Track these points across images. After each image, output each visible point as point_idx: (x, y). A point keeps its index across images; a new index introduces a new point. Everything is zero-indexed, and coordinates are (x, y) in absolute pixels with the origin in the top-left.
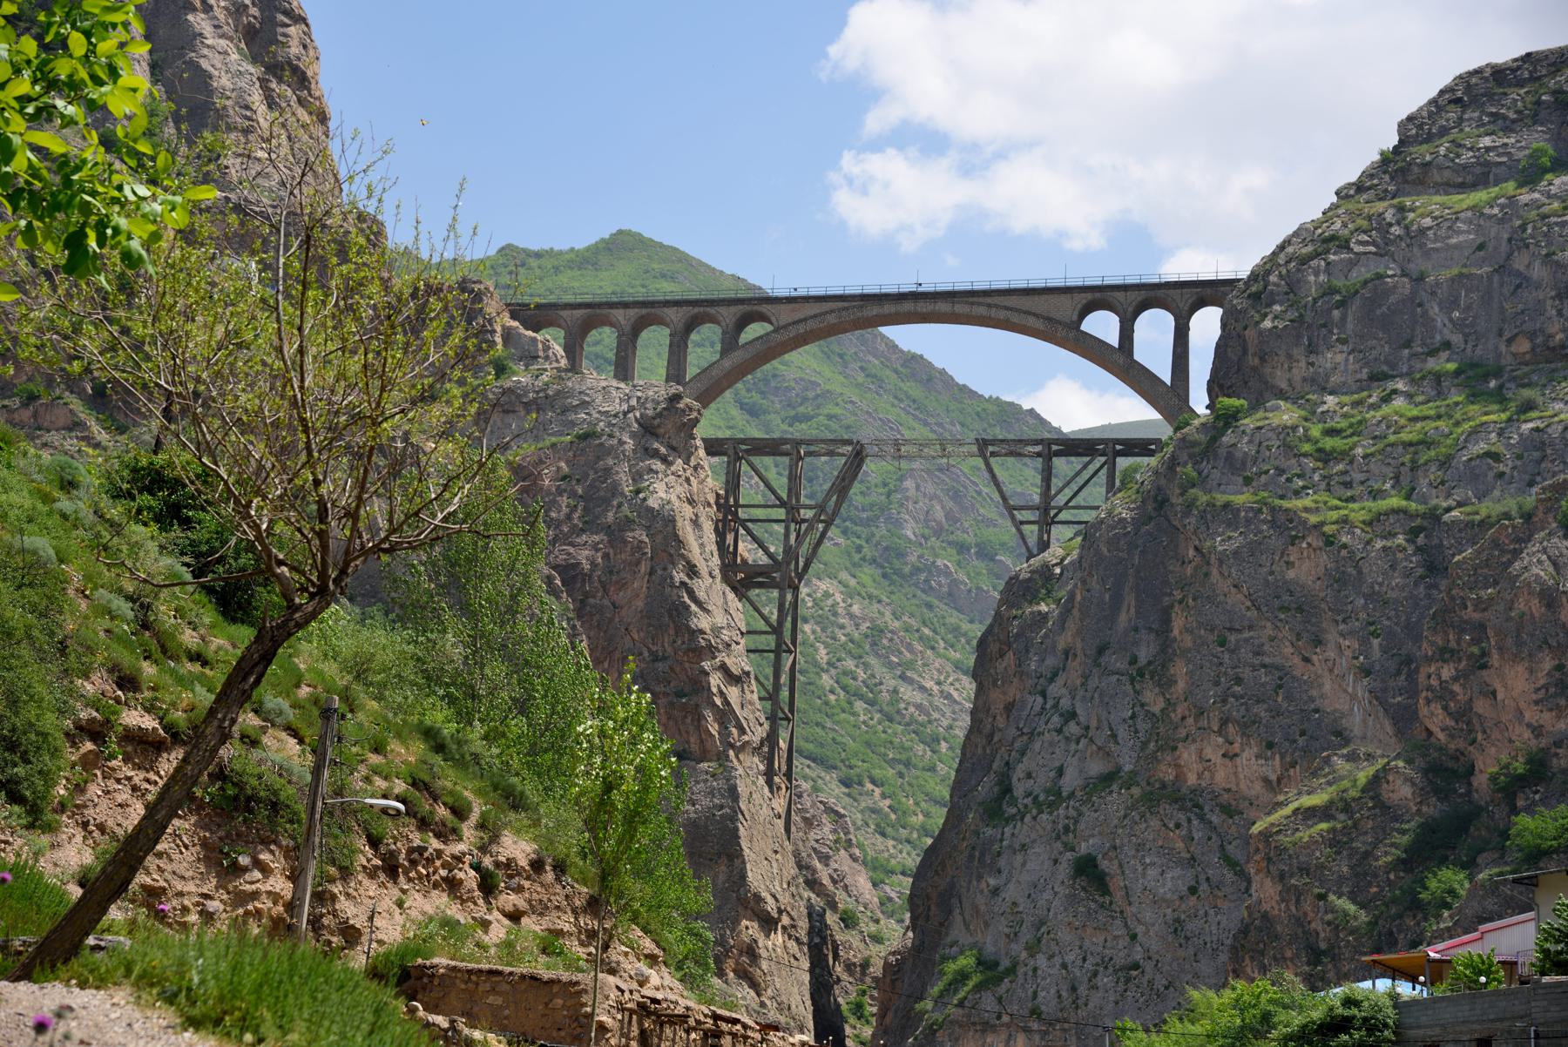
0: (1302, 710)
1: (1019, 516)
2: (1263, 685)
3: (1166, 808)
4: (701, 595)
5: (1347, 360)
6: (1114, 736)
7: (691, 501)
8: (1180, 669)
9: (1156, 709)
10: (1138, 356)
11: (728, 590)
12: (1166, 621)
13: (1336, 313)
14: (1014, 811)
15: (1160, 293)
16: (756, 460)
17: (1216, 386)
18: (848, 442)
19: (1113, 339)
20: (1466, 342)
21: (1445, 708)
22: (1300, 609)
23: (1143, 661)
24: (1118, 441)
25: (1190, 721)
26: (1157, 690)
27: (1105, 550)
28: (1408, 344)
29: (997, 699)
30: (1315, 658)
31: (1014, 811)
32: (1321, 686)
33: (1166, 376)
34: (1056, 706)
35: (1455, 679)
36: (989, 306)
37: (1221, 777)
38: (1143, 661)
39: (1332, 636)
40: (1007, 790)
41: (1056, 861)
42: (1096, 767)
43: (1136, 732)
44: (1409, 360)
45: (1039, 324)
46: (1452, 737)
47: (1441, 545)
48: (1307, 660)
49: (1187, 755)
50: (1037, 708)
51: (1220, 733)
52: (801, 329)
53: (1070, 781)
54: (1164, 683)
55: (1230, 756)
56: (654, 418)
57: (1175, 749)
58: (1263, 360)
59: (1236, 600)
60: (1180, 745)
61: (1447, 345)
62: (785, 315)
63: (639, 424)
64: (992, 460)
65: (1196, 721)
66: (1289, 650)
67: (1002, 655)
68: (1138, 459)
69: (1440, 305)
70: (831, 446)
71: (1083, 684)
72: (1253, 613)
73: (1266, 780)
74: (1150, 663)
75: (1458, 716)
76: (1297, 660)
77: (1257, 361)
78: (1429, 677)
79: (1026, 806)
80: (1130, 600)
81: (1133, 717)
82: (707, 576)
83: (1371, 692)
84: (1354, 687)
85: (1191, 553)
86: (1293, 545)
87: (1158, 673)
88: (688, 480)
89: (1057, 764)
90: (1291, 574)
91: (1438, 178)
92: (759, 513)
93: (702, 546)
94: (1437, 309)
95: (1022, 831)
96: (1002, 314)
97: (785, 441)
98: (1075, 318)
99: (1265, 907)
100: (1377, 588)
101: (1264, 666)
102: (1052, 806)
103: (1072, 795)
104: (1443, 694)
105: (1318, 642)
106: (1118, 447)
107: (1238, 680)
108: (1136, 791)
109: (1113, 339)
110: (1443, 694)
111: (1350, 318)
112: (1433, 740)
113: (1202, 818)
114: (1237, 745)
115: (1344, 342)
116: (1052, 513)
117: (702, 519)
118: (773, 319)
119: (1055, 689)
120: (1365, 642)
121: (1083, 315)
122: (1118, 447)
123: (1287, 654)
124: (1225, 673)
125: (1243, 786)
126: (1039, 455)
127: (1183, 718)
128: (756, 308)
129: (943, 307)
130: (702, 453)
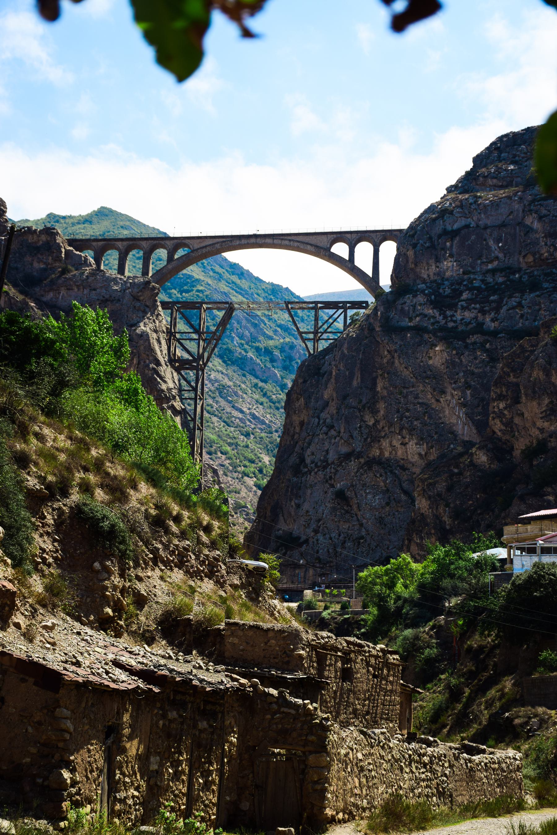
0: (436, 423)
2: (419, 412)
3: (375, 467)
5: (453, 265)
6: (351, 436)
7: (156, 331)
8: (382, 406)
9: (371, 423)
11: (173, 371)
12: (375, 384)
14: (306, 470)
18: (226, 303)
19: (347, 257)
20: (505, 257)
21: (501, 421)
22: (435, 378)
23: (364, 401)
24: (349, 302)
25: (386, 428)
26: (371, 415)
27: (346, 352)
29: (296, 419)
30: (441, 399)
31: (306, 470)
32: (444, 412)
33: (369, 271)
34: (324, 422)
35: (505, 408)
36: (290, 240)
38: (364, 401)
39: (449, 390)
40: (302, 460)
41: (326, 492)
42: (344, 449)
43: (362, 433)
44: (480, 265)
46: (504, 434)
47: (497, 348)
48: (438, 401)
49: (385, 443)
50: (316, 423)
51: (399, 434)
52: (204, 251)
53: (332, 456)
54: (375, 412)
55: (404, 444)
57: (379, 441)
58: (416, 265)
60: (382, 440)
61: (497, 258)
62: (196, 245)
65: (389, 429)
66: (430, 396)
67: (298, 400)
68: (359, 310)
69: (494, 240)
70: (218, 305)
71: (337, 413)
72: (413, 380)
73: (420, 454)
74: (367, 403)
75: (506, 425)
76: (433, 401)
77: (413, 266)
78: (494, 407)
79: (312, 468)
80: (358, 375)
81: (360, 427)
82: (164, 365)
83: (466, 414)
84: (459, 413)
85: (386, 353)
86: (431, 349)
88: (154, 321)
89: (326, 449)
90: (431, 362)
91: (491, 183)
93: (161, 351)
94: (492, 242)
95: (311, 479)
96: (296, 244)
98: (328, 246)
99: (423, 511)
100: (469, 368)
101: (419, 403)
102: (325, 468)
103: (333, 463)
104: (500, 415)
105: (443, 392)
106: (348, 305)
107: (408, 410)
108: (362, 460)
109: (346, 256)
110: (500, 415)
111: (454, 247)
112: (495, 436)
113: (391, 472)
114: (407, 439)
115: (451, 256)
116: (319, 334)
117: (161, 339)
118: (191, 247)
119: (323, 415)
120: (463, 392)
121: (331, 245)
123: (429, 398)
124: (402, 407)
125: (409, 457)
126: (312, 308)
127: (383, 428)
129: (269, 241)
130: (160, 308)
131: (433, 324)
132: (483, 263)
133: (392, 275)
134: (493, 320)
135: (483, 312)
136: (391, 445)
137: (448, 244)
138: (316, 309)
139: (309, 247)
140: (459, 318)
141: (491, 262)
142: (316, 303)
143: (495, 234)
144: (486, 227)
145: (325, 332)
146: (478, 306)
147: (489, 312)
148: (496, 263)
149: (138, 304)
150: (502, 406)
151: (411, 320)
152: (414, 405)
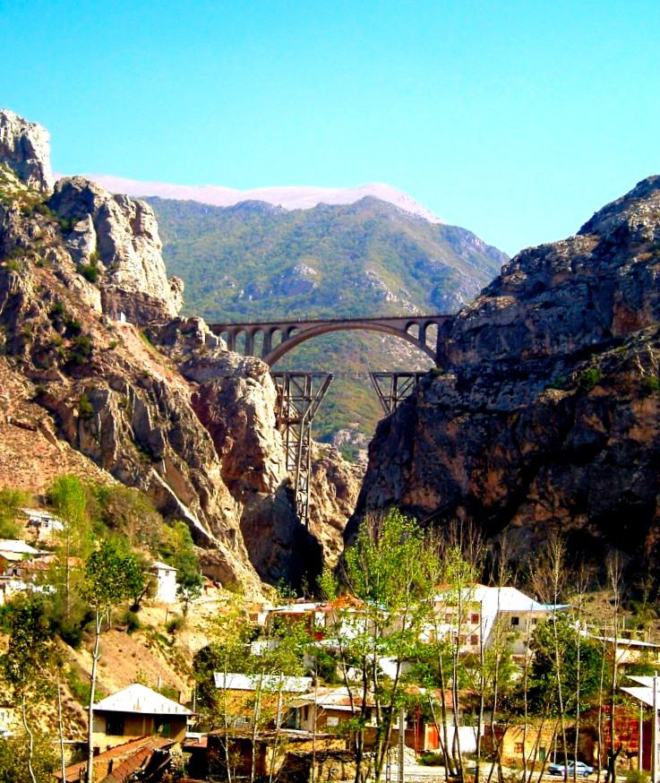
4: (264, 434)
13: (472, 338)
15: (433, 319)
28: (494, 350)
37: (424, 502)
42: (388, 497)
45: (392, 331)
48: (451, 462)
49: (413, 494)
51: (424, 487)
52: (310, 332)
53: (381, 501)
54: (410, 469)
59: (431, 440)
61: (505, 351)
62: (304, 327)
76: (448, 462)
80: (403, 438)
87: (408, 465)
90: (448, 433)
105: (454, 456)
107: (430, 469)
115: (474, 347)
120: (466, 457)
123: (445, 460)
131: (453, 402)
132: (496, 354)
134: (493, 402)
135: (488, 394)
136: (418, 495)
137: (472, 338)
139: (388, 329)
140: (471, 398)
141: (501, 353)
143: (506, 332)
144: (500, 326)
146: (485, 390)
147: (491, 395)
148: (505, 354)
149: (251, 379)
150: (479, 473)
151: (439, 398)
152: (435, 465)
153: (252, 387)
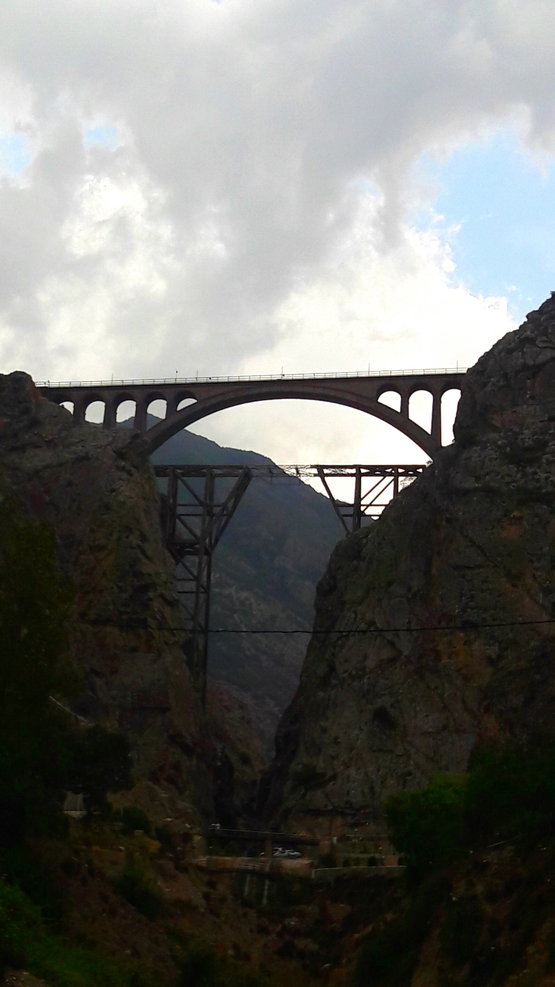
1: (343, 511)
10: (411, 417)
11: (166, 551)
16: (189, 480)
17: (456, 429)
18: (241, 467)
56: (123, 449)
63: (114, 452)
64: (327, 479)
92: (190, 510)
97: (204, 467)
122: (400, 471)
126: (352, 475)
128: (187, 389)
130: (152, 471)
133: (454, 426)
138: (358, 476)
142: (358, 467)
145: (371, 505)
153: (124, 475)
